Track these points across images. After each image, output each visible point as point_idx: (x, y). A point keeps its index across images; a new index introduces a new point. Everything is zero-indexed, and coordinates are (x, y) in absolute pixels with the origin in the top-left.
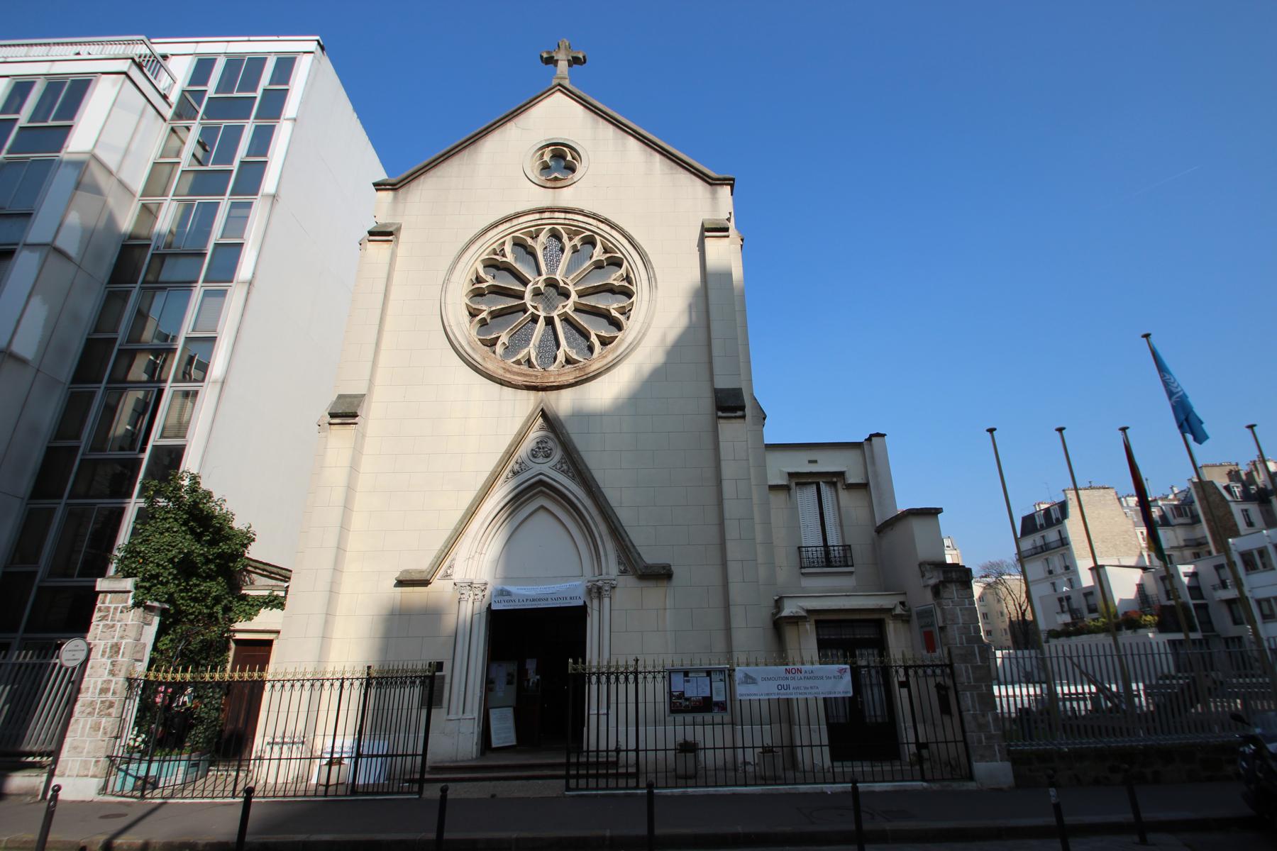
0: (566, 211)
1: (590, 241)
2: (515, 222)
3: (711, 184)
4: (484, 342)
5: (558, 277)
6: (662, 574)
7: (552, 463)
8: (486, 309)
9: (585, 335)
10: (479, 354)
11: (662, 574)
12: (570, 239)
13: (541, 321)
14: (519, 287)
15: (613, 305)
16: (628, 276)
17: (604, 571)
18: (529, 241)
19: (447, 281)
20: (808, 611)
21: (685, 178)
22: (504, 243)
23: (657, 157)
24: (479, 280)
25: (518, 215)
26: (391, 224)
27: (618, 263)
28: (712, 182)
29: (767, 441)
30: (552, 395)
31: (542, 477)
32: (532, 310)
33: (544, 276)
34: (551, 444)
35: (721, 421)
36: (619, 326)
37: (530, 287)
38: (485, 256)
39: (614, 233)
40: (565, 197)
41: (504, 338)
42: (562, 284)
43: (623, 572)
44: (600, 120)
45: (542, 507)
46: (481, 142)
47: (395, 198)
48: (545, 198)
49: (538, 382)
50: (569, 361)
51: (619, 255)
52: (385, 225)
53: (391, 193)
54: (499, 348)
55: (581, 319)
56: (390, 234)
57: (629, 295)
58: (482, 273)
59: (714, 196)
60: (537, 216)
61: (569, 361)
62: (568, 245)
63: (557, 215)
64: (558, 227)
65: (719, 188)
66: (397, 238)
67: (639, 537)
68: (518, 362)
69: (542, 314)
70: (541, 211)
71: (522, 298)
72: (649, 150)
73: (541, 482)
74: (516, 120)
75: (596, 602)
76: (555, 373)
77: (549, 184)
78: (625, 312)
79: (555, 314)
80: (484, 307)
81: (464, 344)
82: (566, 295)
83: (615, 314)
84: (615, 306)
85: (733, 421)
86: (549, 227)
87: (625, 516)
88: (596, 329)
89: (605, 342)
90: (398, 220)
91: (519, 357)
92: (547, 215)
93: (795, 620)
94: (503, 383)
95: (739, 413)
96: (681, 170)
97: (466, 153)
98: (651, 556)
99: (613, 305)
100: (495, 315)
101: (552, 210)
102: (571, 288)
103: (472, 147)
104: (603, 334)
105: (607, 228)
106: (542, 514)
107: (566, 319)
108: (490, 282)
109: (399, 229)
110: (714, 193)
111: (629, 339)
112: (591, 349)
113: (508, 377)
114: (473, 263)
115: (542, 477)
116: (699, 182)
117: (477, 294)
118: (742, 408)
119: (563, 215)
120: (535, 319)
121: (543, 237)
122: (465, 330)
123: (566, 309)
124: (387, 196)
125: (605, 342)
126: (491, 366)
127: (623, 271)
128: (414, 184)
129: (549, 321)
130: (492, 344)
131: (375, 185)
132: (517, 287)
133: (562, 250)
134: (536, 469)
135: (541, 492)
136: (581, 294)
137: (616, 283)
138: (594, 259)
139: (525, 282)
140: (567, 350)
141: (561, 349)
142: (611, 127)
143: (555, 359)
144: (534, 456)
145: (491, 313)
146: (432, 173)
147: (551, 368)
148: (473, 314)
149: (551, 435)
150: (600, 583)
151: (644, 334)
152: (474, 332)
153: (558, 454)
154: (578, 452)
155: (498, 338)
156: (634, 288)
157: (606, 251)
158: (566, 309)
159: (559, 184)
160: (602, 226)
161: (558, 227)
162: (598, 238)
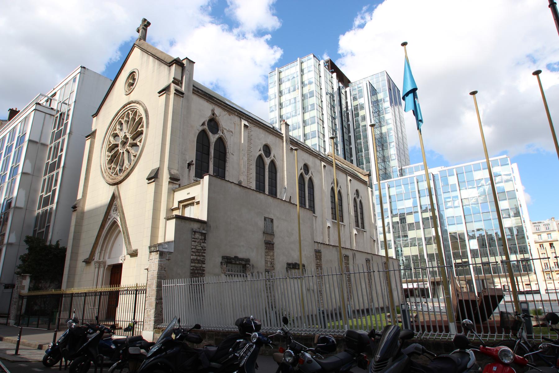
1: (136, 113)
5: (127, 134)
19: (102, 148)
23: (157, 61)
28: (170, 65)
30: (119, 186)
48: (125, 100)
70: (124, 107)
78: (140, 141)
83: (138, 144)
98: (134, 248)
101: (126, 105)
110: (170, 70)
119: (128, 106)
125: (135, 156)
129: (123, 153)
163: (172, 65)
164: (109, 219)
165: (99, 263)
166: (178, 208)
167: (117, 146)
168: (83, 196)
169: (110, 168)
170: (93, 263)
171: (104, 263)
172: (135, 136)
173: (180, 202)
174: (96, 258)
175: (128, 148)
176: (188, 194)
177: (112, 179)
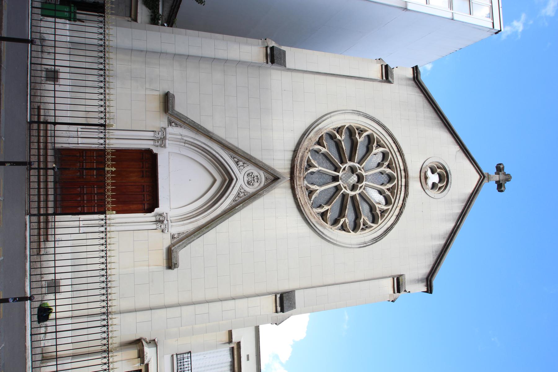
0: (406, 186)
2: (398, 154)
3: (427, 279)
4: (321, 138)
5: (364, 183)
6: (171, 264)
7: (244, 186)
8: (343, 138)
9: (328, 202)
10: (313, 136)
11: (171, 263)
12: (388, 189)
13: (337, 174)
14: (357, 158)
15: (348, 219)
16: (367, 227)
17: (173, 224)
18: (386, 163)
20: (147, 365)
21: (430, 261)
22: (385, 147)
23: (443, 242)
24: (361, 131)
25: (402, 155)
26: (392, 78)
27: (374, 220)
29: (261, 328)
31: (235, 180)
32: (343, 167)
33: (364, 174)
34: (256, 184)
35: (274, 297)
36: (335, 222)
37: (357, 165)
38: (375, 136)
39: (394, 218)
40: (415, 185)
41: (323, 150)
42: (360, 185)
43: (173, 237)
44: (464, 204)
45: (215, 181)
46: (446, 130)
47: (409, 79)
48: (414, 172)
49: (297, 173)
50: (311, 193)
51: (380, 221)
52: (392, 74)
53: (411, 76)
54: (318, 147)
55: (338, 198)
56: (387, 77)
57: (355, 228)
58: (365, 134)
59: (419, 281)
60: (402, 168)
61: (311, 193)
62: (384, 188)
63: (403, 180)
64: (396, 182)
65: (425, 284)
66: (385, 82)
67: (197, 244)
68: (309, 160)
69: (340, 174)
70: (406, 170)
71: (350, 160)
72: (447, 236)
73: (231, 180)
74: (461, 151)
75: (154, 219)
76: (301, 183)
77: (423, 174)
78: (343, 228)
79: (340, 182)
80: (343, 137)
81: (320, 126)
82: (354, 188)
83: (342, 221)
84: (347, 221)
85: (274, 305)
86: (395, 175)
87: (210, 235)
88: (333, 209)
89: (323, 215)
90: (395, 81)
91: (312, 161)
92: (403, 174)
93: (141, 355)
94: (295, 151)
95: (279, 309)
96: (436, 258)
97: (439, 121)
99: (348, 219)
100: (338, 145)
101: (406, 177)
102: (358, 192)
103: (442, 124)
104: (329, 214)
105: (397, 213)
106: (210, 180)
107: (338, 189)
108: (359, 140)
109: (390, 82)
111: (325, 232)
112: (320, 206)
113: (300, 155)
114: (372, 128)
115: (235, 180)
116: (427, 270)
117: (351, 132)
118: (282, 311)
119: (403, 184)
120: (337, 169)
121: (388, 171)
122: (329, 125)
123: (344, 190)
124: (410, 74)
125: (323, 215)
126: (305, 143)
127: (370, 223)
128: (417, 90)
130: (319, 143)
131: (416, 67)
132: (357, 158)
133: (382, 184)
134: (240, 176)
135: (225, 180)
136: (353, 198)
137: (362, 220)
138: (377, 206)
139: (360, 162)
140: (318, 192)
141: (317, 188)
142: (460, 211)
143: (312, 184)
144: (248, 175)
145: (340, 141)
146: (425, 101)
147: (306, 182)
148: (339, 130)
149: (262, 185)
150: (165, 222)
151: (329, 241)
152: (325, 131)
153: (250, 190)
154: (252, 202)
155: (324, 147)
156: (359, 232)
157: (383, 212)
158: (344, 190)
159: (423, 180)
160: (398, 209)
161: (396, 182)
162: (390, 207)
163: (427, 286)
164: (237, 163)
165: (164, 139)
166: (230, 341)
167: (351, 159)
168: (289, 70)
169: (319, 143)
170: (164, 122)
171: (163, 146)
172: (356, 204)
173: (239, 344)
174: (174, 131)
175: (342, 192)
176: (248, 359)
177: (302, 157)
